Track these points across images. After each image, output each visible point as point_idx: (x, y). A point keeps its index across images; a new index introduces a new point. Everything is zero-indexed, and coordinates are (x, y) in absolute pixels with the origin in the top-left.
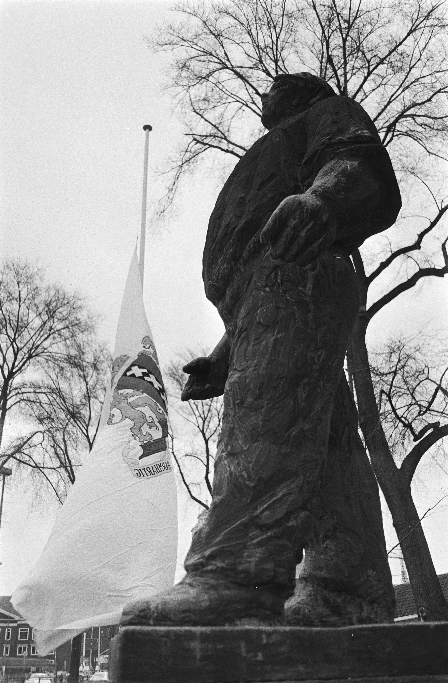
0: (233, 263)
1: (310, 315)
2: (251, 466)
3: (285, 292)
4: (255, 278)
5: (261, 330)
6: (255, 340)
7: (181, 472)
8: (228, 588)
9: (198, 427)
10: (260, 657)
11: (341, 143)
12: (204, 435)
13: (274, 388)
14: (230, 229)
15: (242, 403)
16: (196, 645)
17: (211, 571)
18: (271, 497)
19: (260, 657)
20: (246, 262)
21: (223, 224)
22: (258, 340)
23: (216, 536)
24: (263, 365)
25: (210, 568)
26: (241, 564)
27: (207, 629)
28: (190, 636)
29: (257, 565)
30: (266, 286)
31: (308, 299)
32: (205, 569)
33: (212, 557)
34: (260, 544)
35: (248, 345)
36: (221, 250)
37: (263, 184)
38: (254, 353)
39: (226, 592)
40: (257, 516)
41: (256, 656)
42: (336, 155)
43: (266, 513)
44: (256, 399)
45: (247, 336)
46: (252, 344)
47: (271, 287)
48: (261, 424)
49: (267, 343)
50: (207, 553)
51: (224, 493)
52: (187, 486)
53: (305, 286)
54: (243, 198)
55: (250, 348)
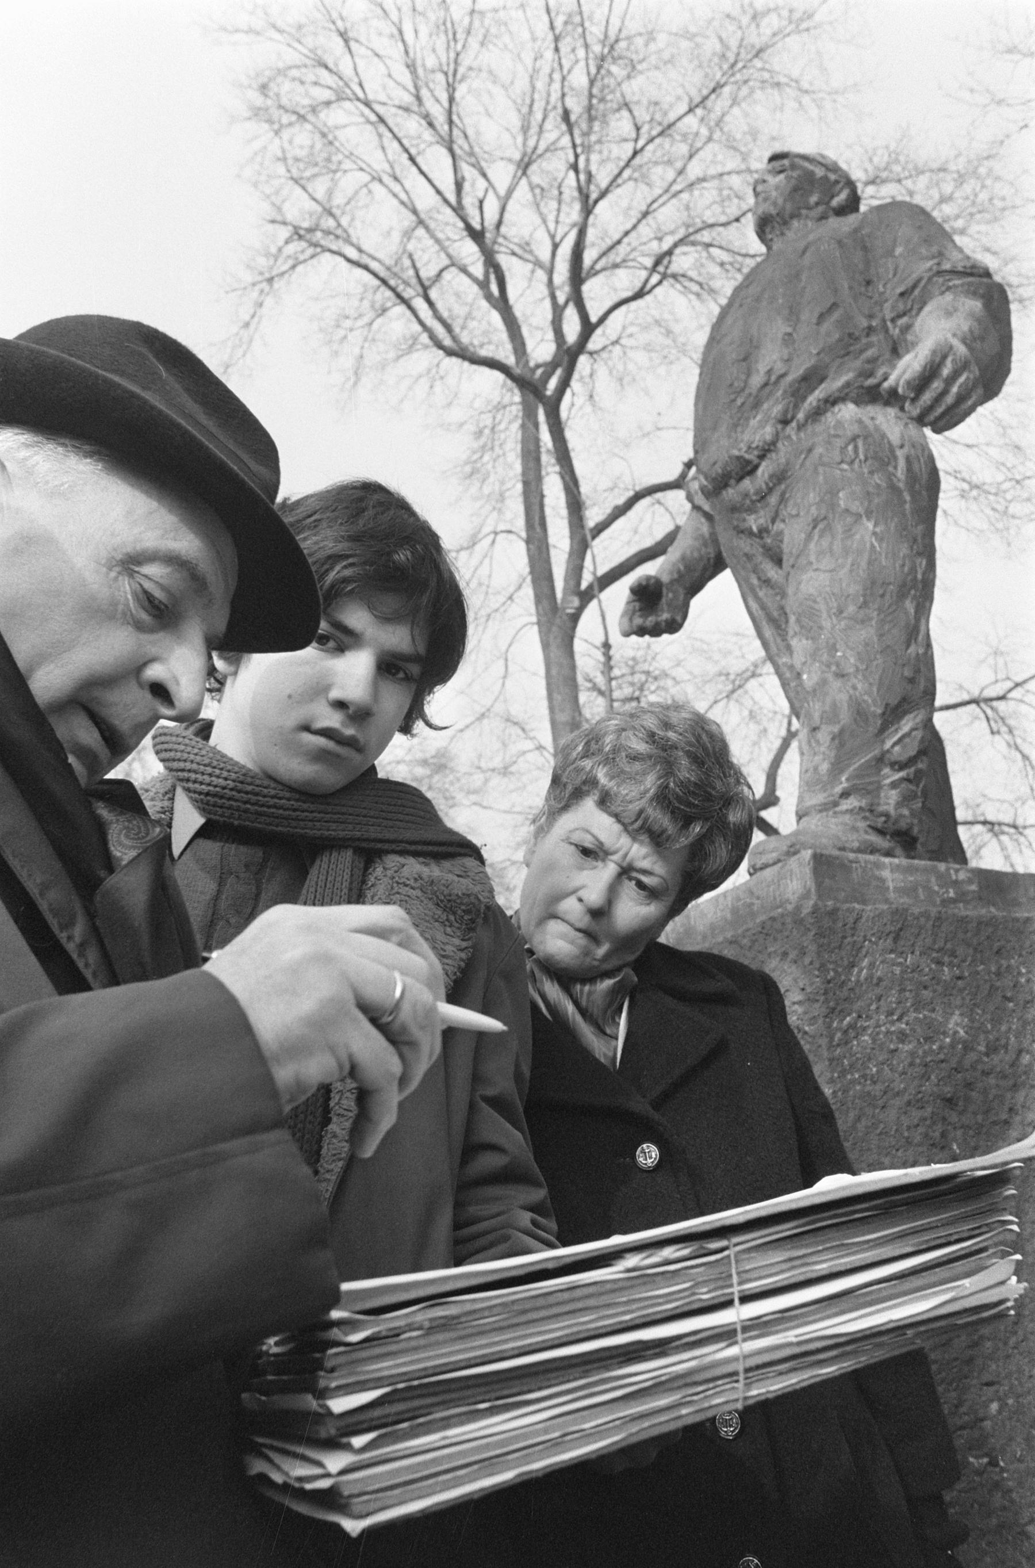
0: (779, 427)
2: (875, 689)
3: (871, 473)
6: (845, 532)
10: (952, 894)
13: (882, 596)
14: (773, 378)
15: (841, 612)
16: (886, 874)
17: (850, 811)
18: (896, 731)
19: (952, 894)
20: (800, 427)
21: (762, 367)
22: (848, 532)
24: (864, 564)
26: (879, 804)
31: (901, 485)
32: (837, 809)
33: (845, 794)
34: (894, 785)
35: (833, 537)
36: (757, 405)
37: (822, 317)
38: (846, 551)
39: (868, 837)
40: (888, 751)
41: (947, 892)
42: (949, 288)
43: (897, 748)
45: (829, 528)
46: (840, 536)
48: (875, 639)
50: (838, 789)
53: (895, 468)
54: (790, 334)
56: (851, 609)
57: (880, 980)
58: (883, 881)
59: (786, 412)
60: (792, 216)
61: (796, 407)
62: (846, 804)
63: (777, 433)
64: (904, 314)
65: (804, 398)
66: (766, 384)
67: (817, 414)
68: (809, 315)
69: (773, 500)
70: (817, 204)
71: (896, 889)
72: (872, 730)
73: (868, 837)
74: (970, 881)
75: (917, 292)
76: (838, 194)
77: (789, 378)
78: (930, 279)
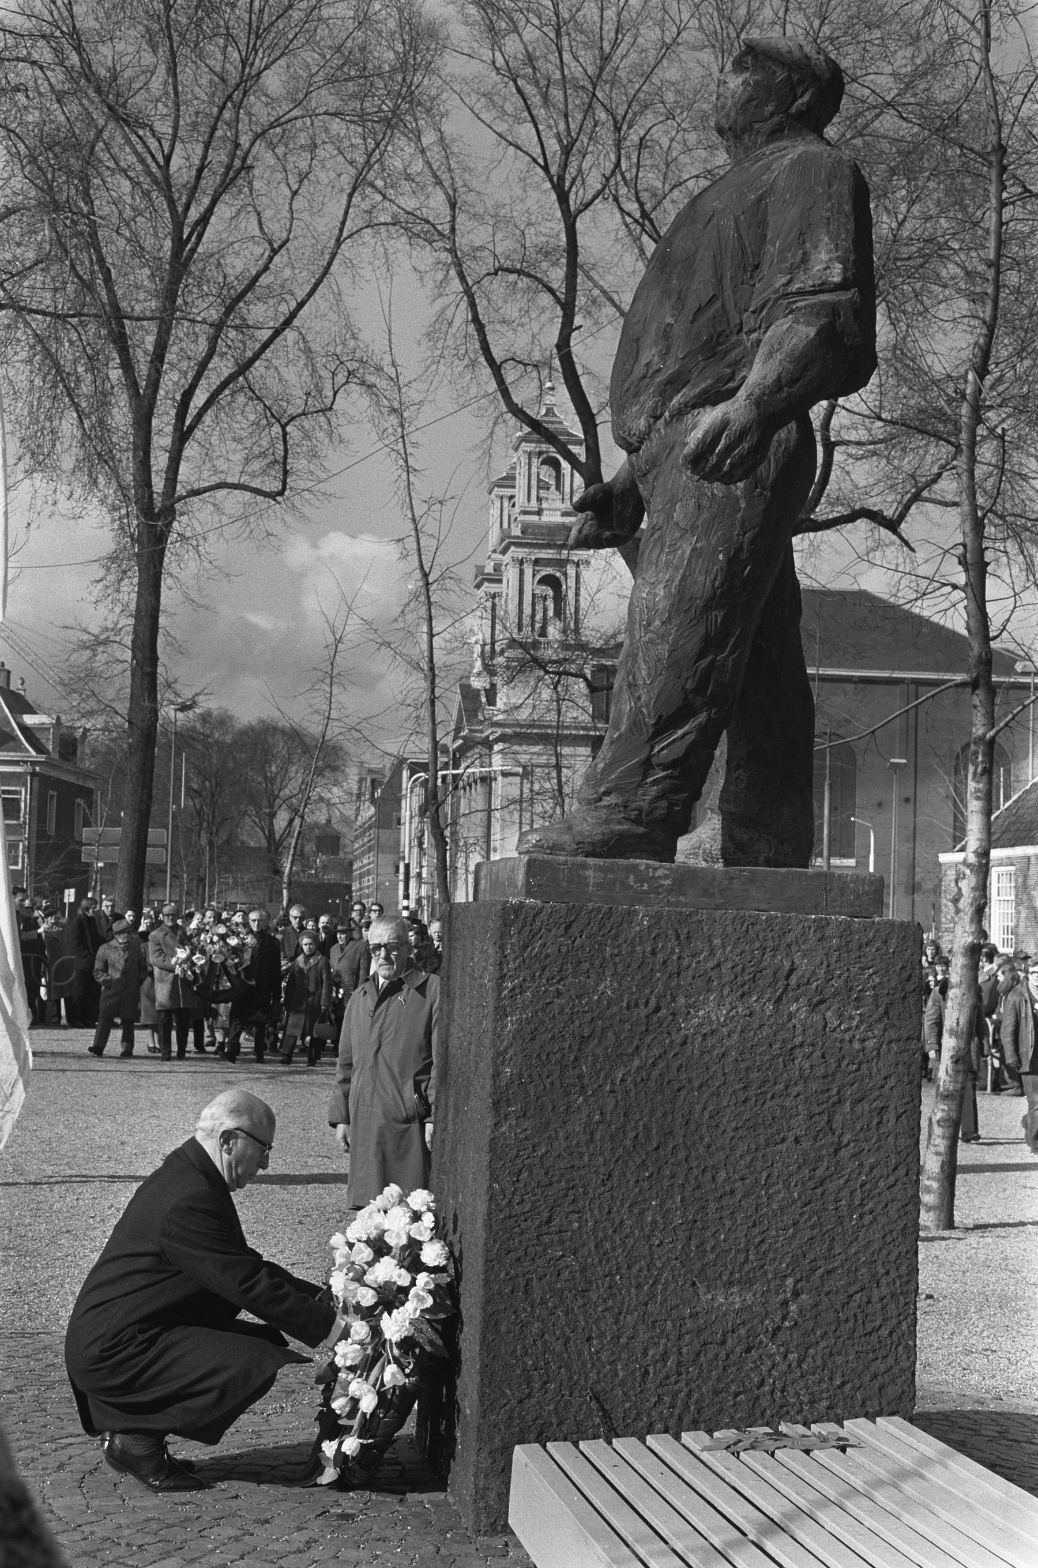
1: (739, 515)
5: (677, 534)
7: (476, 319)
8: (620, 823)
9: (546, 168)
10: (646, 887)
11: (801, 293)
12: (563, 198)
16: (590, 873)
21: (644, 361)
23: (612, 772)
25: (603, 803)
27: (601, 862)
28: (584, 866)
29: (652, 802)
34: (655, 782)
35: (662, 550)
36: (637, 394)
39: (620, 827)
42: (791, 312)
44: (663, 623)
49: (683, 553)
50: (602, 789)
51: (623, 728)
52: (496, 368)
55: (663, 557)
56: (657, 623)
57: (547, 956)
58: (586, 878)
59: (655, 408)
60: (744, 131)
62: (606, 801)
63: (650, 426)
64: (755, 331)
66: (644, 377)
70: (772, 115)
71: (596, 884)
72: (645, 737)
73: (620, 827)
74: (666, 877)
76: (802, 96)
78: (777, 300)
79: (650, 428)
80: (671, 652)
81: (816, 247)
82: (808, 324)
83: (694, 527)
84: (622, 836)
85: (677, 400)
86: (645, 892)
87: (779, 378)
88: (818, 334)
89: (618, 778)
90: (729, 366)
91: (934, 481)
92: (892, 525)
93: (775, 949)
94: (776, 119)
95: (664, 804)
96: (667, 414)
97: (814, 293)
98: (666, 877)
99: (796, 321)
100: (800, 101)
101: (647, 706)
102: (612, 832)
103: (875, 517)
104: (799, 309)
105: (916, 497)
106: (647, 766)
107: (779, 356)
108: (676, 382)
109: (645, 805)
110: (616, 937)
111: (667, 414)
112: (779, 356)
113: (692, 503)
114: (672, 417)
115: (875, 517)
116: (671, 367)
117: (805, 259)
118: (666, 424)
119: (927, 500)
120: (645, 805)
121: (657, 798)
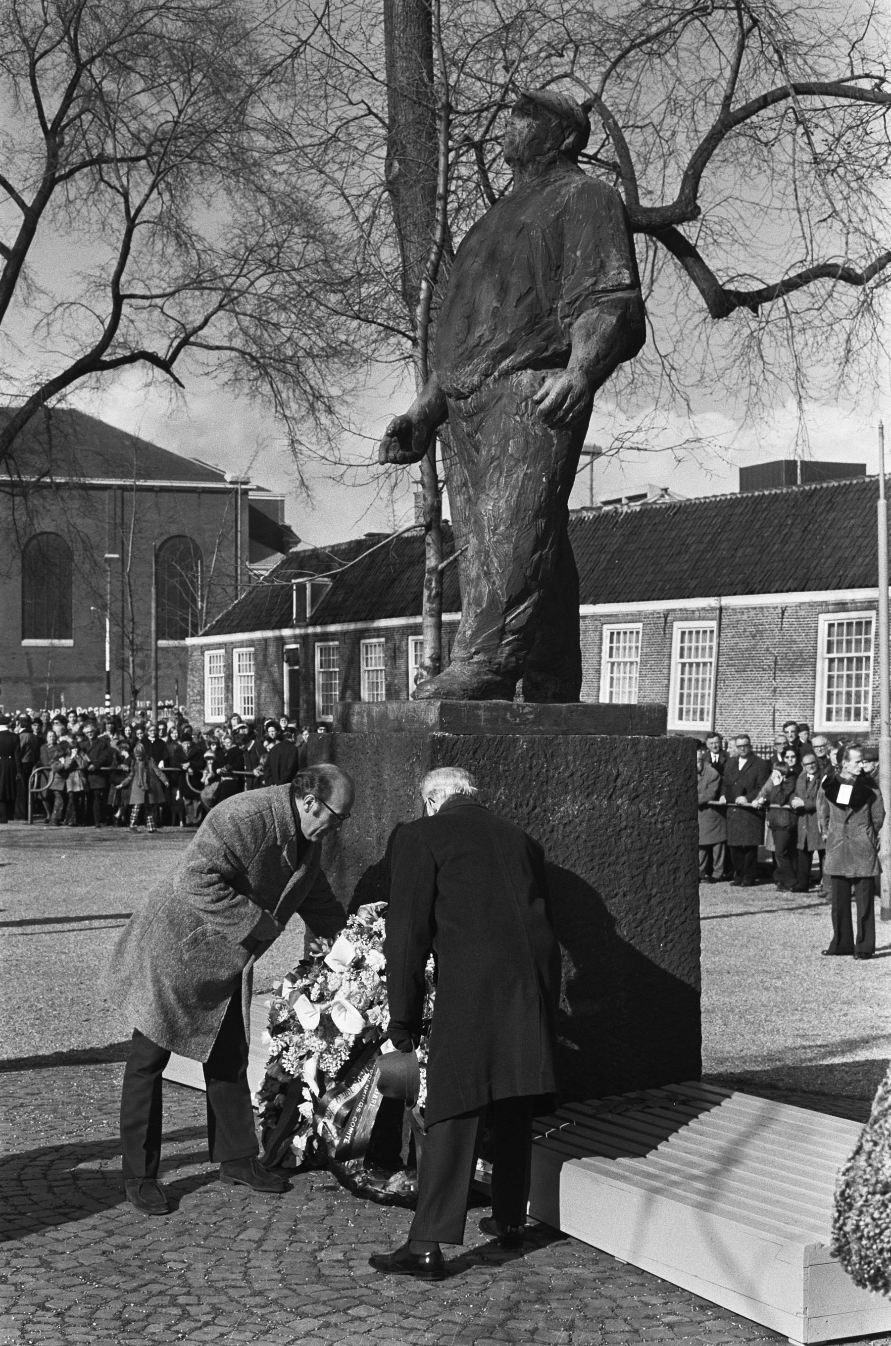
4: (504, 400)
8: (486, 674)
11: (605, 291)
15: (496, 529)
16: (481, 712)
23: (479, 637)
28: (477, 707)
30: (517, 414)
33: (476, 653)
34: (508, 644)
35: (501, 475)
36: (470, 358)
42: (598, 304)
47: (522, 416)
50: (473, 650)
55: (503, 480)
56: (502, 528)
59: (487, 369)
60: (528, 161)
61: (494, 367)
62: (476, 658)
64: (568, 316)
65: (500, 363)
66: (478, 345)
67: (507, 374)
68: (512, 298)
69: (476, 419)
70: (549, 150)
72: (500, 611)
74: (531, 713)
75: (578, 303)
77: (493, 347)
78: (587, 296)
79: (481, 383)
80: (515, 549)
81: (608, 257)
82: (610, 314)
83: (525, 458)
84: (489, 682)
85: (504, 364)
86: (517, 724)
87: (598, 354)
88: (618, 321)
89: (483, 641)
90: (544, 340)
91: (201, 328)
92: (165, 365)
93: (607, 761)
94: (551, 154)
95: (513, 659)
96: (496, 374)
97: (613, 291)
98: (531, 713)
99: (602, 311)
100: (567, 141)
101: (501, 588)
102: (483, 682)
103: (152, 358)
104: (603, 302)
105: (185, 342)
106: (502, 633)
107: (595, 338)
108: (505, 352)
109: (502, 660)
110: (506, 758)
111: (496, 374)
112: (595, 338)
113: (521, 440)
114: (500, 376)
115: (152, 358)
116: (501, 340)
117: (602, 266)
118: (495, 380)
119: (194, 344)
120: (502, 660)
121: (510, 655)
